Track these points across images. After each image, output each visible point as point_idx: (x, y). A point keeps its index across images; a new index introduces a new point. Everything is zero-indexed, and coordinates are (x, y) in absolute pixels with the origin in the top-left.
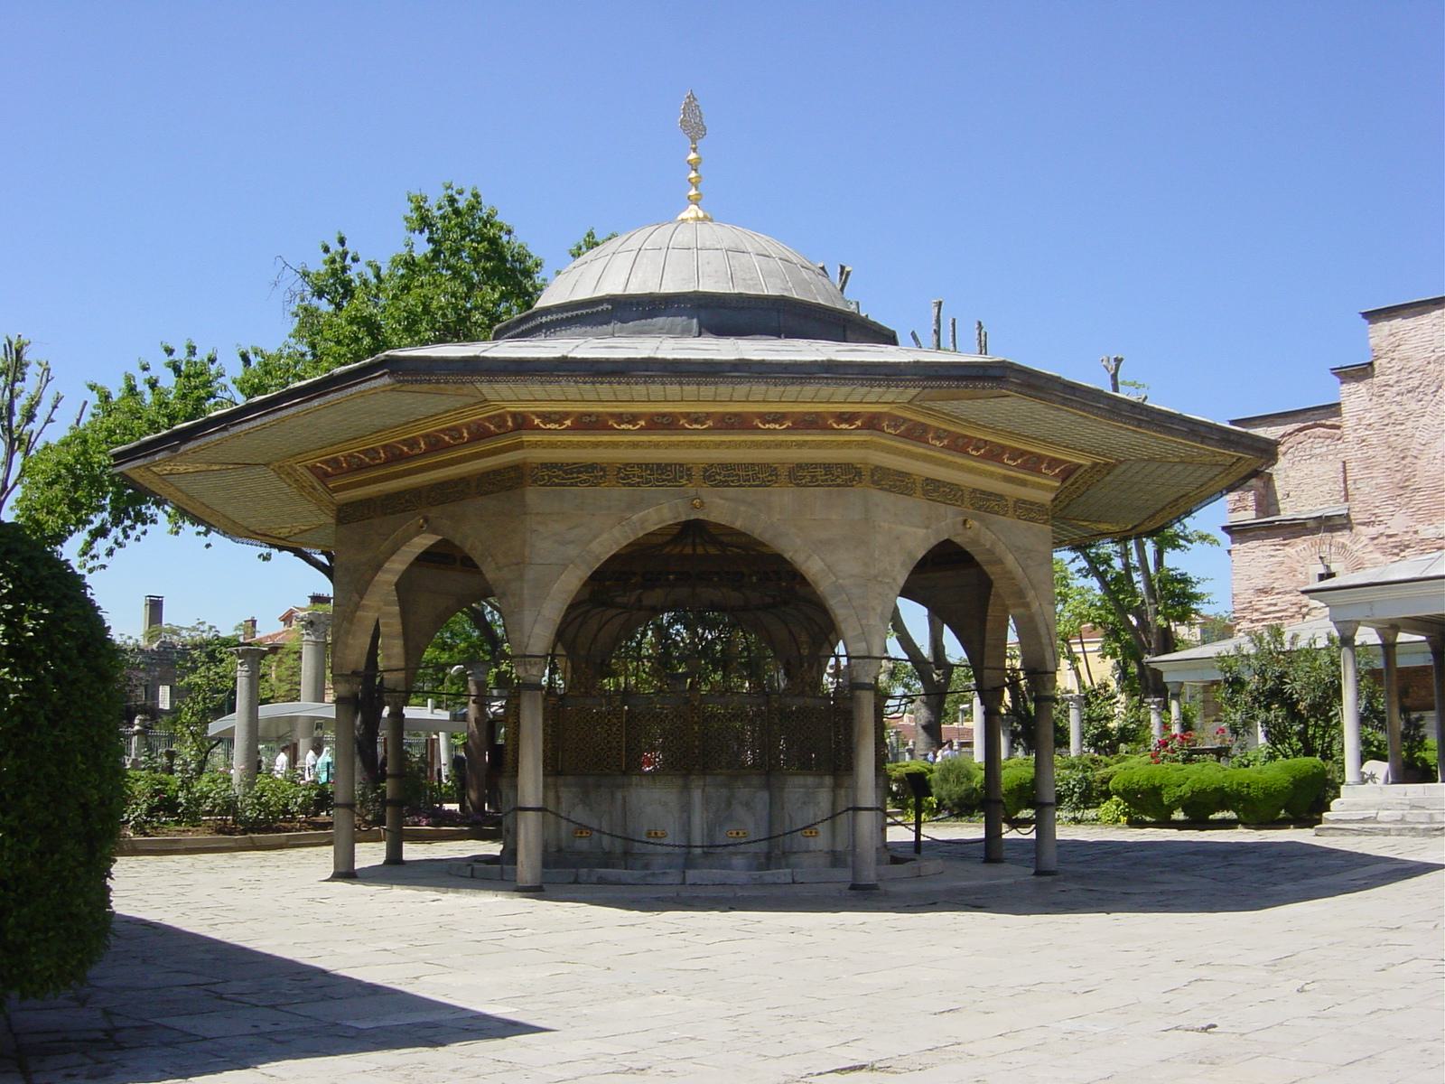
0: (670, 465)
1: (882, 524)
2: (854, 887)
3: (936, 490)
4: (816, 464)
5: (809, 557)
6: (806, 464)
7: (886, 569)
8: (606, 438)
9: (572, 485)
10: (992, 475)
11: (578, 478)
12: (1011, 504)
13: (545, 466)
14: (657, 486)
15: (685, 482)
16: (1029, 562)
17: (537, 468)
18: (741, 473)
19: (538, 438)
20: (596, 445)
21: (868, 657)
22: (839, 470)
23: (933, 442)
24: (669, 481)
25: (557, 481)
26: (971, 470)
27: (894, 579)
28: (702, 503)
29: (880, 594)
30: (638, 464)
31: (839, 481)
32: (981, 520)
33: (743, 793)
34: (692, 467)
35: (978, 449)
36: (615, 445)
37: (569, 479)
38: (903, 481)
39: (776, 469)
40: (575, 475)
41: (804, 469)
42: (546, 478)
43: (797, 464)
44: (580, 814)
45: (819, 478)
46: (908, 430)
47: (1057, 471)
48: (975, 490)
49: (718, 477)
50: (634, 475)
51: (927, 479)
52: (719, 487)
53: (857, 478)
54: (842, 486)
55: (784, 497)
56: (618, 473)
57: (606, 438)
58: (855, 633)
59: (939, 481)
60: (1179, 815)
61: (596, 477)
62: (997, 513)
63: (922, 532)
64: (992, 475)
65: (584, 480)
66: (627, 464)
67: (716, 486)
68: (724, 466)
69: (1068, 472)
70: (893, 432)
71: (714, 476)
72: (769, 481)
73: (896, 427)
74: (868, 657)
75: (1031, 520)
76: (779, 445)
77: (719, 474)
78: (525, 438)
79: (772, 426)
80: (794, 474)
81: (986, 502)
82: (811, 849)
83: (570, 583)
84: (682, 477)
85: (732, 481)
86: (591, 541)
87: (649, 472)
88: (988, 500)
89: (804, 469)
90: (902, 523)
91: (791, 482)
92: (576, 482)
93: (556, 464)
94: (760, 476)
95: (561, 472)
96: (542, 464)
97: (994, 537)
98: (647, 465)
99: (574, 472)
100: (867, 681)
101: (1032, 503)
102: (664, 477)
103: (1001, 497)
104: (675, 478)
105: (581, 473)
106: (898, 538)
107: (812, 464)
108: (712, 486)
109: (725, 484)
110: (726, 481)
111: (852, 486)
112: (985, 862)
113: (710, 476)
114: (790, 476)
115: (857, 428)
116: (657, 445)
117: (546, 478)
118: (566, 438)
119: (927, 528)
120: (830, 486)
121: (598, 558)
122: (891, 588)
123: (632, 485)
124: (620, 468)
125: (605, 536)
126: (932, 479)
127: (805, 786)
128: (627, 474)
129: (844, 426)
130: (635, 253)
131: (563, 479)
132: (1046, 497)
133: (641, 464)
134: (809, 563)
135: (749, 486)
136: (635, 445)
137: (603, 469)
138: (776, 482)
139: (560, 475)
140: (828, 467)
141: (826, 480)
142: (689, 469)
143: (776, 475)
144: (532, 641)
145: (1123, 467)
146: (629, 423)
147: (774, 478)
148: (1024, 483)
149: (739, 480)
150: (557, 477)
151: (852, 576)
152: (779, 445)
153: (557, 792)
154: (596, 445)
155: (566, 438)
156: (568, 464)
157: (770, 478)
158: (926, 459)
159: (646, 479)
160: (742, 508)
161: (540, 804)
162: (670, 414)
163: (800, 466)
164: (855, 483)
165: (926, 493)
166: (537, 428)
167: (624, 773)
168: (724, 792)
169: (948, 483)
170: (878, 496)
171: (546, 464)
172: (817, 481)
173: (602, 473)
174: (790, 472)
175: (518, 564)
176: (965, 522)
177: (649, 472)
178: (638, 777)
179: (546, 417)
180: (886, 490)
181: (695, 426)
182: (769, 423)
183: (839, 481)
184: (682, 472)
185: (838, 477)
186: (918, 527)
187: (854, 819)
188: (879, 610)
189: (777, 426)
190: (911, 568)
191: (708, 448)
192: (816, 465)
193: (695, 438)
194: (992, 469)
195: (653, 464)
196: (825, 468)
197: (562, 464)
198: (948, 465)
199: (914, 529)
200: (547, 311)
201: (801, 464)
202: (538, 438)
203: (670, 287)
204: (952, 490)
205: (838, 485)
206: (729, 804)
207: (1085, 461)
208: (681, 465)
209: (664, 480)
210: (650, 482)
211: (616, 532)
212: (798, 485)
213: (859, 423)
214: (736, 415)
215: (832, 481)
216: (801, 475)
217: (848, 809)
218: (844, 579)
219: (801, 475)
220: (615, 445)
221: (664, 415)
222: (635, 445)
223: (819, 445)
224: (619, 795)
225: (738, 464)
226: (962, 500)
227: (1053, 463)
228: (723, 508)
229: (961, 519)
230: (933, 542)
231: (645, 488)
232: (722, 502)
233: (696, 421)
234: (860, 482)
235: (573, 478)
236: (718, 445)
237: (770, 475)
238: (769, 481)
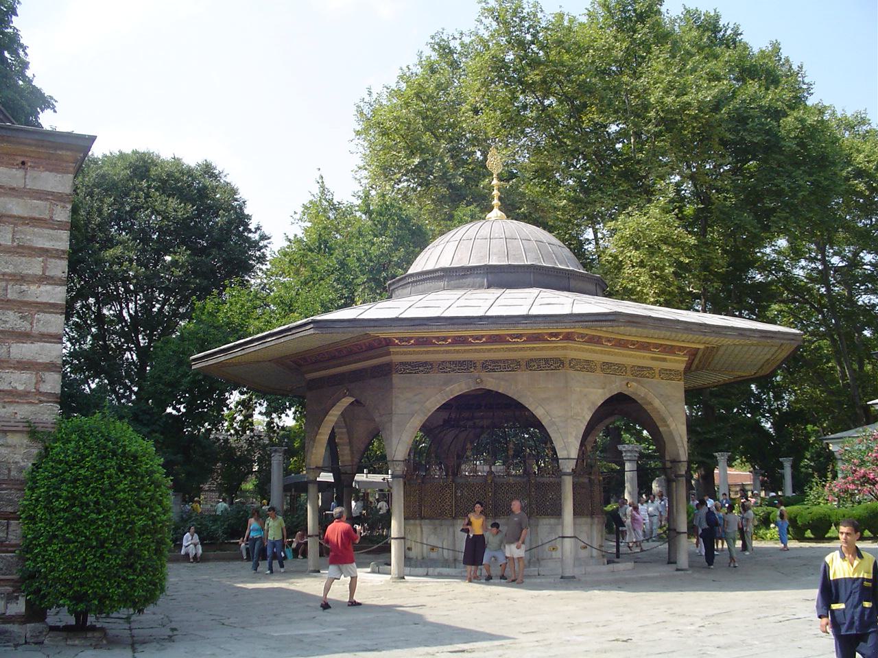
0: (465, 361)
2: (562, 578)
3: (607, 367)
5: (537, 407)
8: (431, 349)
9: (415, 373)
12: (657, 371)
13: (402, 363)
16: (669, 402)
19: (398, 350)
20: (427, 352)
21: (568, 459)
24: (465, 370)
26: (630, 356)
27: (584, 417)
28: (482, 381)
29: (575, 426)
32: (638, 382)
35: (634, 345)
36: (437, 352)
44: (433, 541)
46: (589, 338)
47: (685, 352)
48: (634, 366)
51: (604, 363)
55: (523, 376)
57: (431, 349)
60: (809, 534)
63: (601, 391)
68: (494, 361)
69: (693, 353)
70: (581, 340)
73: (582, 338)
74: (568, 459)
75: (671, 379)
76: (521, 349)
79: (516, 340)
81: (641, 372)
82: (554, 557)
83: (417, 421)
84: (471, 368)
86: (425, 402)
90: (588, 388)
98: (453, 362)
100: (568, 471)
103: (651, 368)
106: (585, 395)
109: (493, 370)
112: (668, 563)
113: (486, 366)
115: (561, 340)
116: (458, 352)
119: (603, 388)
121: (429, 411)
122: (581, 422)
123: (447, 372)
125: (433, 399)
127: (549, 524)
128: (443, 366)
129: (554, 339)
130: (458, 242)
132: (682, 367)
136: (447, 352)
137: (431, 364)
140: (547, 360)
143: (519, 365)
145: (724, 348)
146: (443, 341)
148: (664, 360)
151: (559, 417)
152: (521, 349)
153: (421, 528)
154: (427, 352)
156: (413, 363)
160: (502, 383)
161: (403, 536)
162: (464, 336)
163: (532, 360)
165: (603, 370)
166: (397, 344)
167: (454, 518)
170: (571, 372)
176: (627, 384)
179: (401, 340)
180: (578, 370)
182: (515, 338)
186: (599, 389)
187: (562, 542)
188: (574, 434)
190: (594, 411)
192: (540, 359)
193: (477, 347)
198: (616, 354)
199: (595, 390)
200: (412, 275)
202: (398, 350)
203: (473, 263)
205: (552, 369)
207: (702, 347)
208: (471, 361)
211: (438, 397)
212: (531, 370)
213: (561, 337)
214: (497, 335)
216: (531, 364)
217: (560, 537)
219: (531, 364)
220: (437, 352)
221: (460, 337)
222: (447, 352)
223: (542, 349)
224: (451, 530)
226: (626, 373)
227: (681, 349)
228: (494, 382)
229: (625, 383)
230: (608, 396)
231: (452, 373)
232: (491, 380)
233: (477, 339)
236: (489, 350)
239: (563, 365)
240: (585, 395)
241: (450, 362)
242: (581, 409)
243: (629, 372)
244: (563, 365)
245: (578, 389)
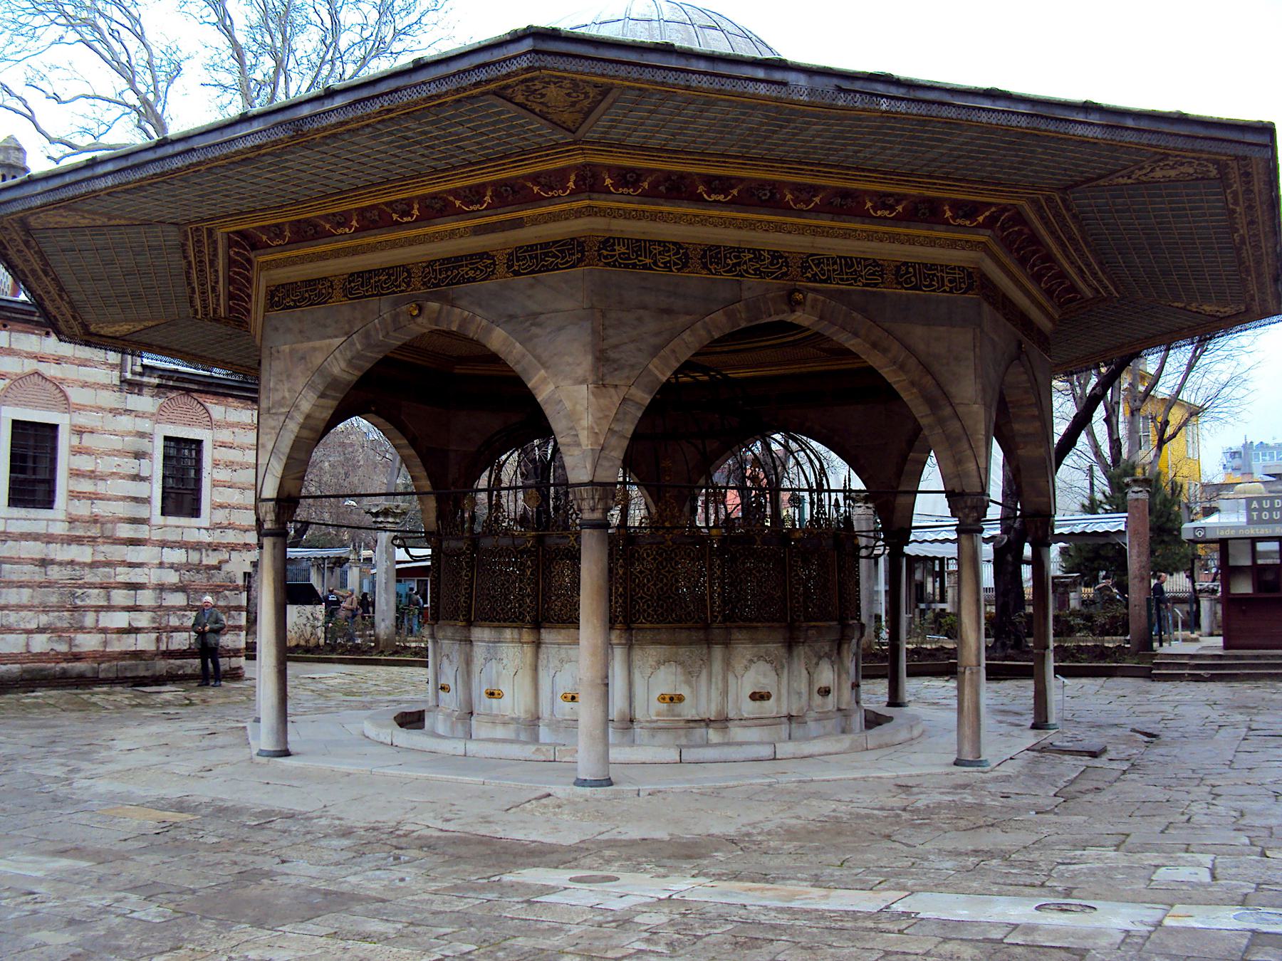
1: (282, 348)
7: (284, 398)
10: (452, 234)
16: (534, 330)
23: (340, 231)
26: (411, 242)
38: (315, 290)
48: (431, 263)
51: (352, 275)
59: (370, 271)
62: (474, 280)
70: (281, 242)
88: (462, 266)
97: (466, 313)
101: (546, 245)
103: (483, 255)
126: (358, 273)
148: (518, 224)
158: (336, 254)
165: (348, 293)
169: (384, 269)
180: (290, 307)
194: (450, 226)
198: (372, 248)
199: (327, 341)
204: (389, 275)
226: (408, 285)
240: (303, 358)
242: (289, 391)
243: (416, 281)
245: (286, 348)
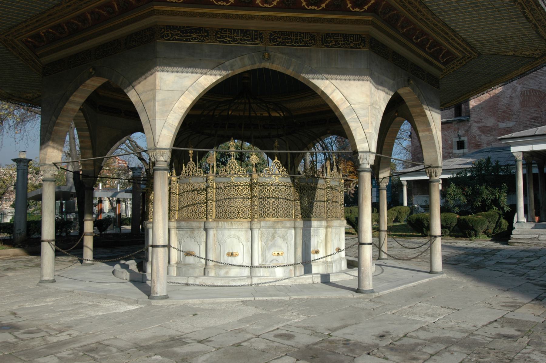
4: (338, 34)
6: (332, 34)
9: (186, 40)
11: (190, 36)
14: (241, 43)
15: (258, 42)
17: (164, 28)
18: (293, 38)
22: (352, 38)
25: (177, 37)
30: (229, 29)
31: (352, 45)
33: (281, 231)
34: (263, 33)
37: (185, 36)
39: (314, 36)
40: (189, 34)
41: (331, 37)
42: (170, 35)
43: (327, 34)
45: (340, 42)
49: (278, 40)
50: (226, 37)
52: (280, 45)
53: (362, 43)
54: (354, 48)
56: (216, 34)
58: (362, 137)
61: (202, 36)
64: (420, 56)
65: (195, 38)
66: (222, 29)
67: (278, 45)
71: (276, 39)
72: (310, 43)
77: (280, 38)
78: (156, 8)
79: (313, 7)
80: (325, 40)
84: (256, 39)
85: (288, 43)
87: (236, 35)
89: (331, 37)
91: (323, 45)
92: (189, 39)
93: (177, 27)
94: (305, 40)
95: (179, 32)
96: (167, 26)
98: (235, 30)
99: (188, 33)
102: (245, 38)
104: (252, 39)
105: (193, 33)
107: (335, 34)
108: (275, 45)
110: (284, 42)
111: (360, 48)
113: (274, 39)
114: (322, 40)
115: (365, 11)
116: (241, 17)
117: (170, 35)
118: (182, 9)
120: (346, 47)
124: (217, 32)
131: (181, 36)
133: (231, 29)
134: (334, 94)
135: (298, 46)
136: (227, 16)
137: (206, 31)
138: (314, 44)
139: (179, 34)
140: (346, 36)
141: (344, 44)
142: (260, 34)
144: (161, 139)
147: (313, 41)
148: (431, 64)
149: (291, 42)
150: (176, 35)
154: (203, 15)
155: (182, 9)
156: (184, 27)
157: (310, 42)
159: (234, 38)
163: (328, 35)
164: (361, 46)
168: (272, 231)
171: (170, 26)
172: (339, 44)
173: (206, 34)
174: (322, 38)
175: (151, 90)
177: (236, 35)
178: (222, 222)
181: (266, 5)
183: (352, 45)
184: (257, 35)
185: (351, 42)
189: (316, 8)
191: (273, 20)
195: (238, 30)
196: (343, 37)
197: (180, 27)
201: (329, 34)
205: (351, 47)
206: (273, 237)
209: (245, 40)
210: (237, 41)
212: (327, 46)
215: (347, 45)
218: (355, 104)
225: (291, 32)
234: (364, 46)
235: (187, 36)
237: (311, 40)
238: (310, 43)
239: (365, 44)
241: (230, 30)
244: (365, 44)
